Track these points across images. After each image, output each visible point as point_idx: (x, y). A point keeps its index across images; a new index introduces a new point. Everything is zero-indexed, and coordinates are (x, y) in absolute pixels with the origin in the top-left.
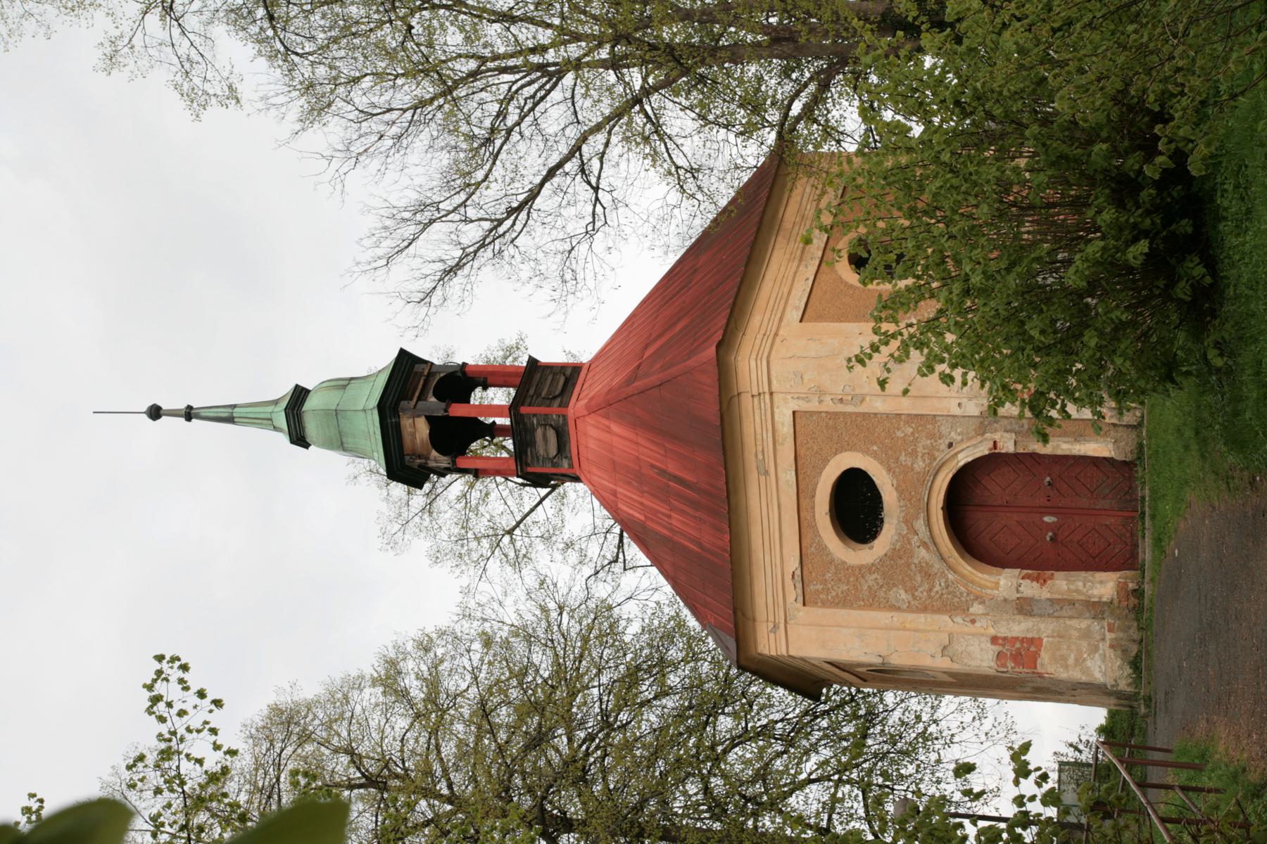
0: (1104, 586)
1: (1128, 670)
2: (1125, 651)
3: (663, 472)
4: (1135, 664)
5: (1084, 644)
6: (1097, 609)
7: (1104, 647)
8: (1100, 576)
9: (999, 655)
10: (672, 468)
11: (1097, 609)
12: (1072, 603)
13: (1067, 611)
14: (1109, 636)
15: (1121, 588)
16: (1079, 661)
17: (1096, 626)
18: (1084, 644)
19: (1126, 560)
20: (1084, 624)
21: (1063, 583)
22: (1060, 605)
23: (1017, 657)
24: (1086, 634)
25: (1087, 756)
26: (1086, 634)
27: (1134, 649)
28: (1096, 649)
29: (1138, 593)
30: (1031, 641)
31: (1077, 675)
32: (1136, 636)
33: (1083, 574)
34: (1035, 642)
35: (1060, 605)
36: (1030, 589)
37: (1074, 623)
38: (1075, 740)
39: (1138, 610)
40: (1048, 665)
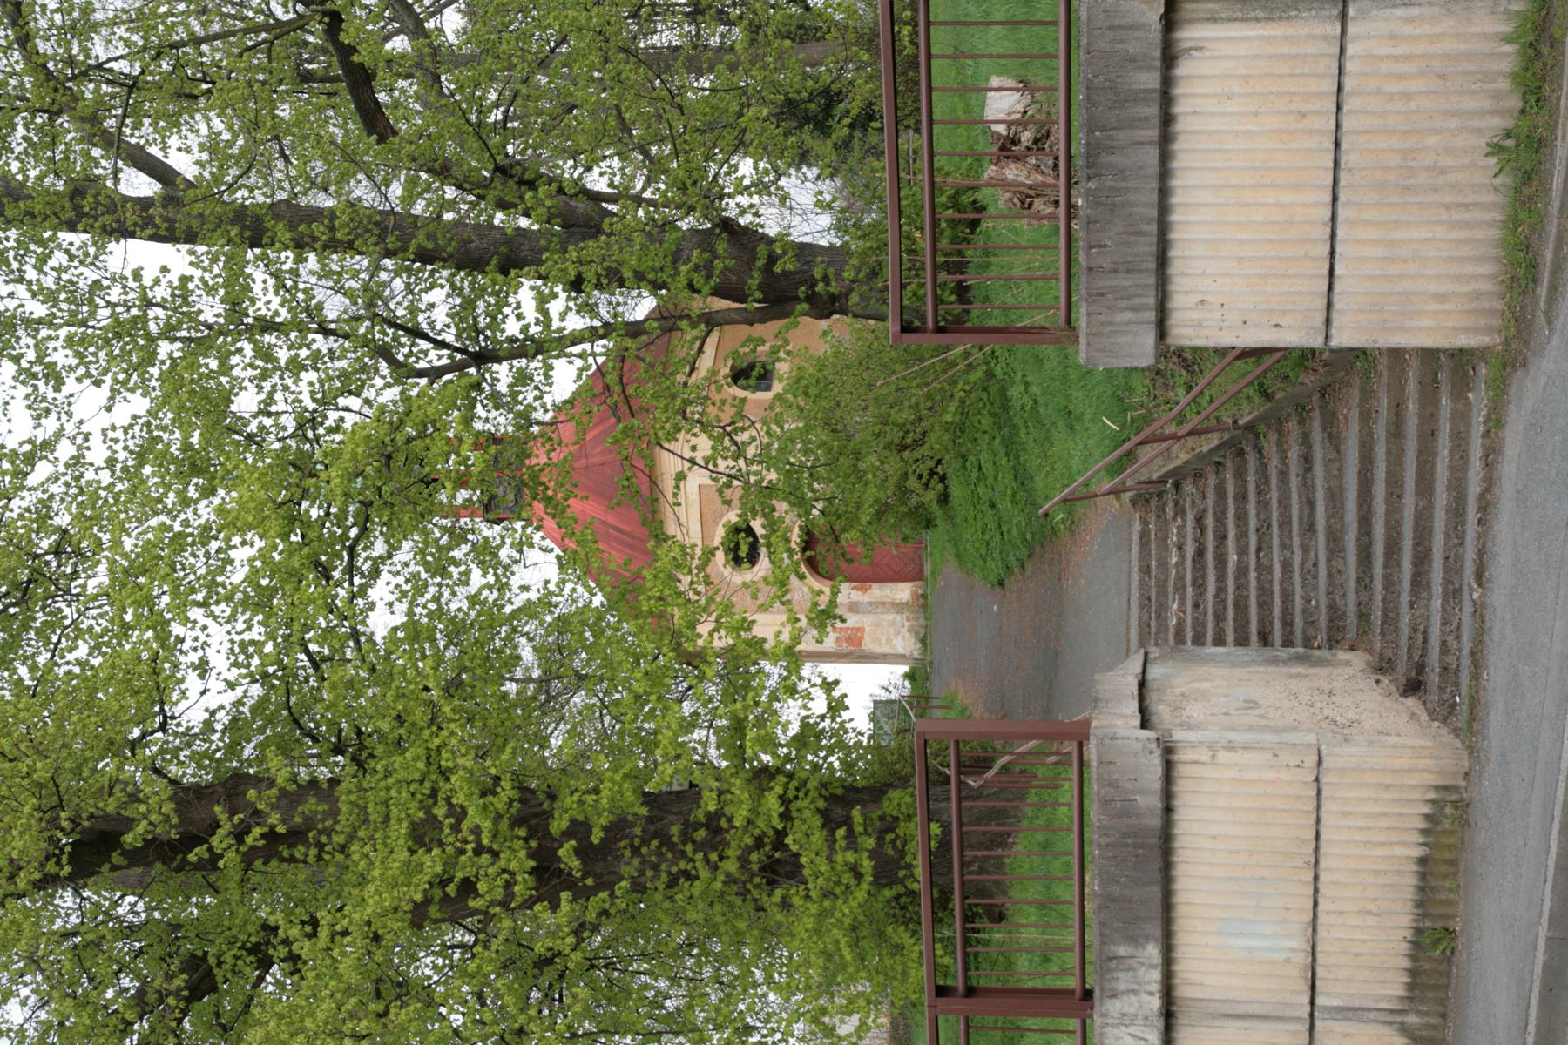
0: (903, 592)
1: (919, 645)
2: (917, 633)
3: (604, 523)
4: (923, 641)
5: (891, 630)
6: (899, 607)
7: (904, 631)
8: (901, 585)
9: (838, 639)
10: (612, 520)
11: (899, 607)
12: (883, 604)
13: (881, 609)
14: (907, 624)
15: (914, 593)
16: (889, 641)
17: (898, 617)
18: (891, 630)
19: (916, 576)
20: (891, 617)
21: (877, 591)
22: (877, 605)
23: (849, 640)
24: (893, 623)
25: (894, 695)
26: (893, 623)
27: (922, 632)
28: (899, 632)
29: (924, 596)
30: (858, 629)
31: (886, 649)
32: (923, 622)
33: (890, 585)
34: (860, 630)
35: (877, 605)
36: (857, 596)
37: (885, 616)
38: (886, 683)
39: (924, 607)
40: (869, 645)
